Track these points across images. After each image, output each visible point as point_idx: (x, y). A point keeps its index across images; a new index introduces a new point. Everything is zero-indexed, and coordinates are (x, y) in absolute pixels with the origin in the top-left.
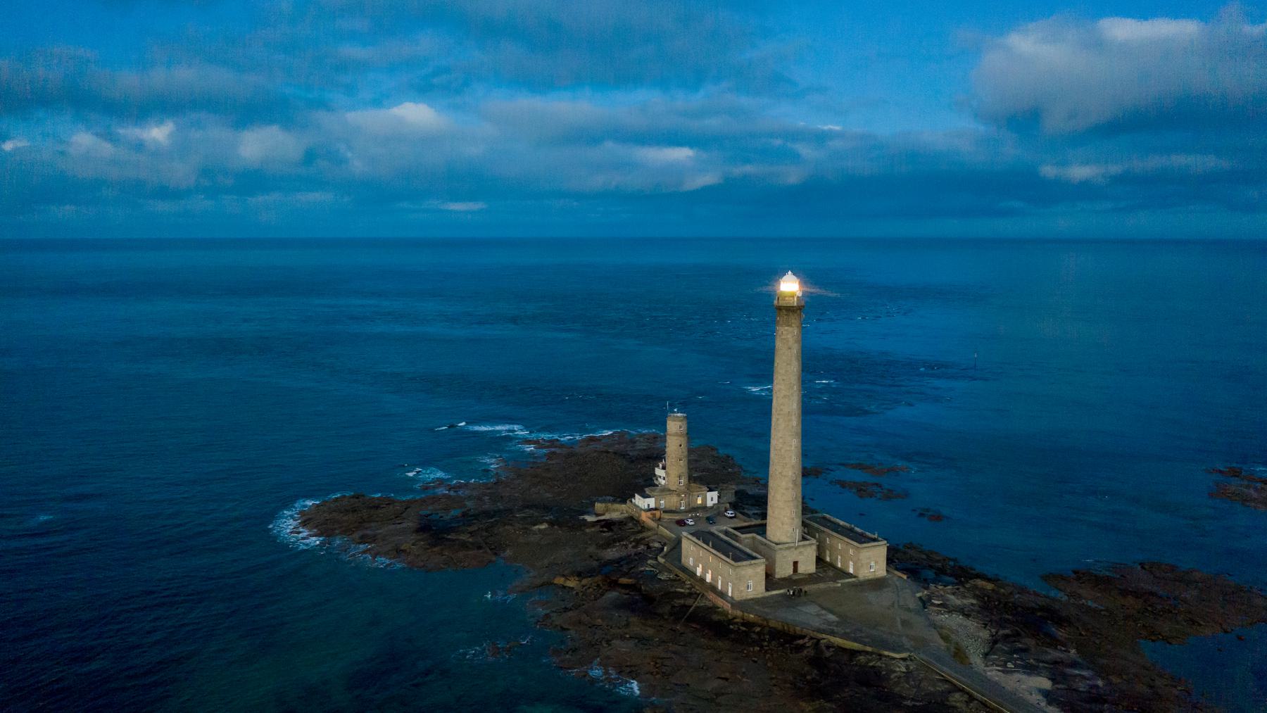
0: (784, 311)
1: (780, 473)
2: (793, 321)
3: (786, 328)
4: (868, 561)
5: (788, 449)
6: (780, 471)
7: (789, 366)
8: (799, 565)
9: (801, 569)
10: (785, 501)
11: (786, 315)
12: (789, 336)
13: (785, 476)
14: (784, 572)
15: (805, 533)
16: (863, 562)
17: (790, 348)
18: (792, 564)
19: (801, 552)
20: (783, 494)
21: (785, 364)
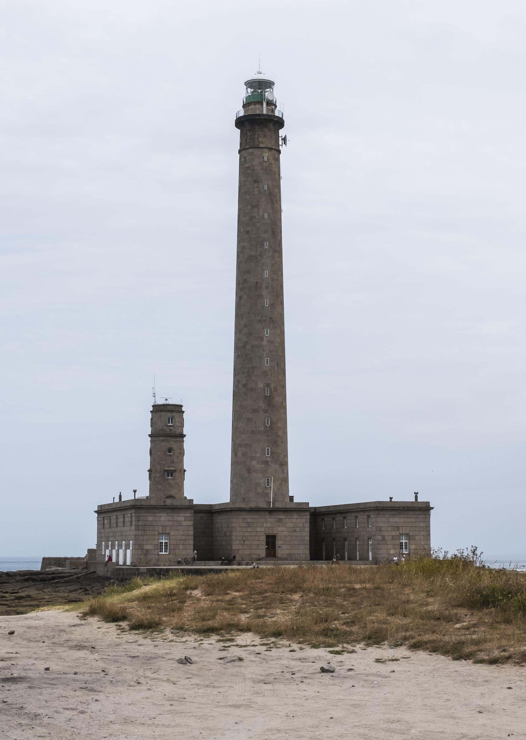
0: (247, 124)
1: (244, 385)
2: (260, 139)
3: (251, 150)
4: (394, 533)
5: (256, 343)
6: (244, 382)
7: (255, 210)
8: (278, 543)
9: (282, 550)
10: (253, 432)
11: (250, 130)
12: (254, 163)
13: (252, 390)
14: (247, 552)
15: (441, 633)
16: (384, 533)
17: (256, 181)
18: (264, 538)
19: (280, 520)
20: (249, 419)
21: (249, 207)
